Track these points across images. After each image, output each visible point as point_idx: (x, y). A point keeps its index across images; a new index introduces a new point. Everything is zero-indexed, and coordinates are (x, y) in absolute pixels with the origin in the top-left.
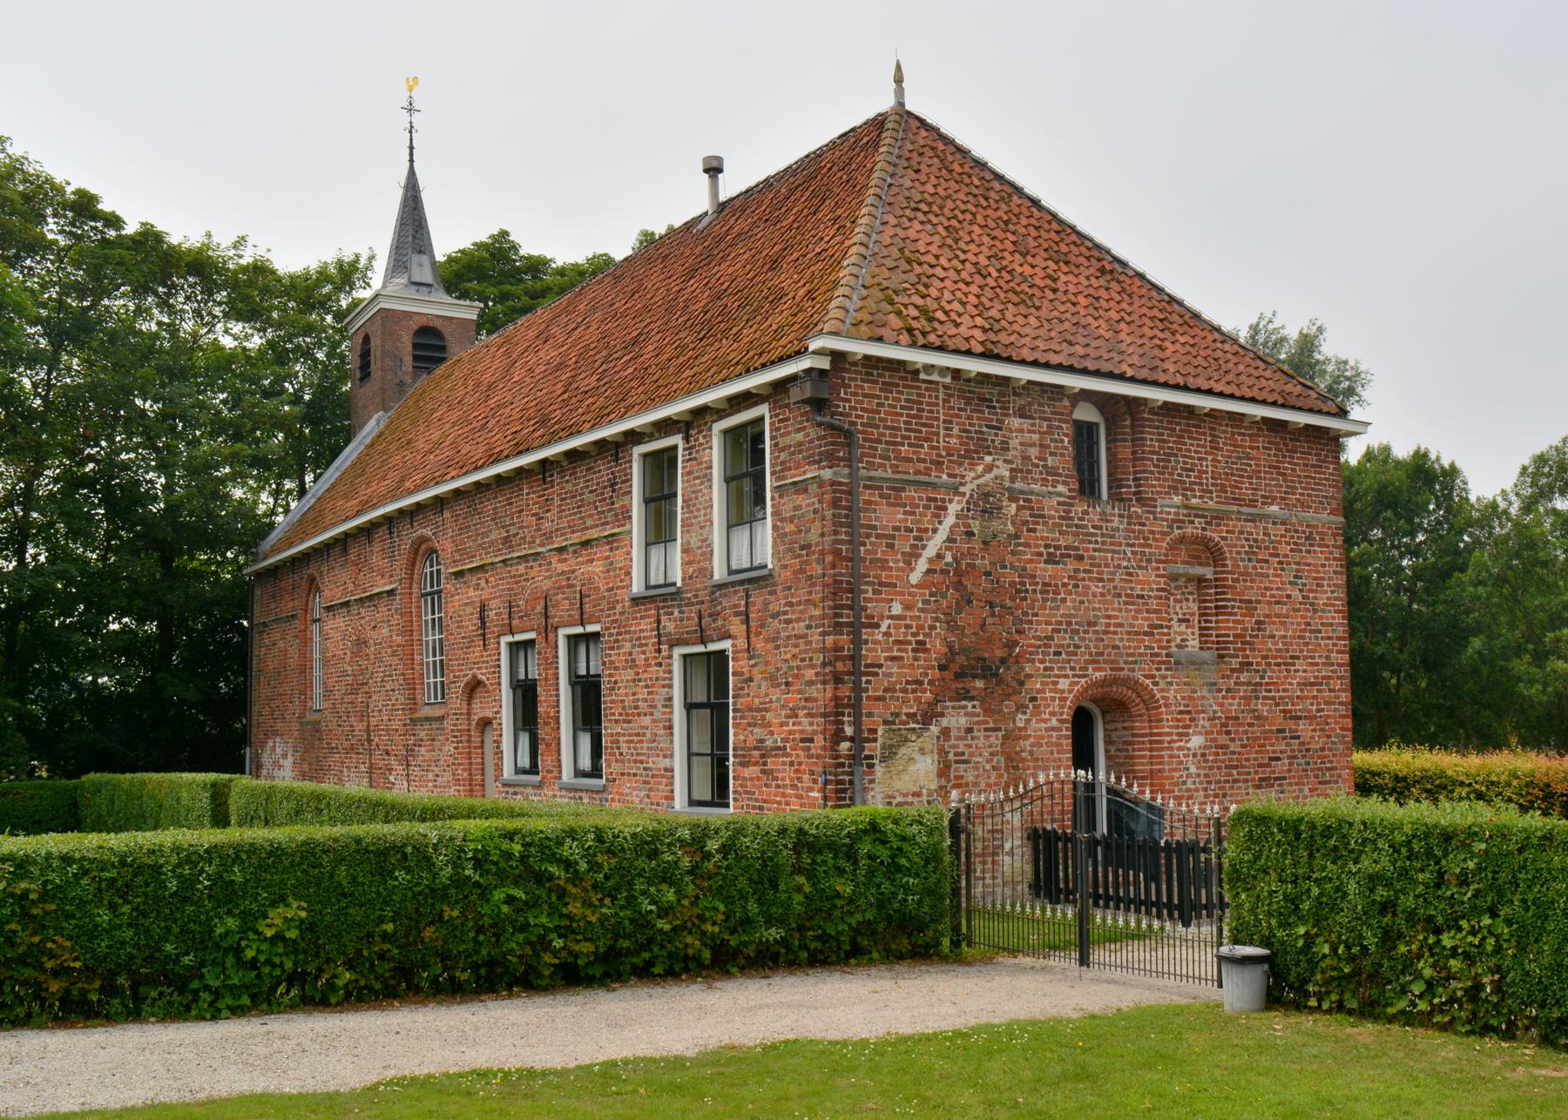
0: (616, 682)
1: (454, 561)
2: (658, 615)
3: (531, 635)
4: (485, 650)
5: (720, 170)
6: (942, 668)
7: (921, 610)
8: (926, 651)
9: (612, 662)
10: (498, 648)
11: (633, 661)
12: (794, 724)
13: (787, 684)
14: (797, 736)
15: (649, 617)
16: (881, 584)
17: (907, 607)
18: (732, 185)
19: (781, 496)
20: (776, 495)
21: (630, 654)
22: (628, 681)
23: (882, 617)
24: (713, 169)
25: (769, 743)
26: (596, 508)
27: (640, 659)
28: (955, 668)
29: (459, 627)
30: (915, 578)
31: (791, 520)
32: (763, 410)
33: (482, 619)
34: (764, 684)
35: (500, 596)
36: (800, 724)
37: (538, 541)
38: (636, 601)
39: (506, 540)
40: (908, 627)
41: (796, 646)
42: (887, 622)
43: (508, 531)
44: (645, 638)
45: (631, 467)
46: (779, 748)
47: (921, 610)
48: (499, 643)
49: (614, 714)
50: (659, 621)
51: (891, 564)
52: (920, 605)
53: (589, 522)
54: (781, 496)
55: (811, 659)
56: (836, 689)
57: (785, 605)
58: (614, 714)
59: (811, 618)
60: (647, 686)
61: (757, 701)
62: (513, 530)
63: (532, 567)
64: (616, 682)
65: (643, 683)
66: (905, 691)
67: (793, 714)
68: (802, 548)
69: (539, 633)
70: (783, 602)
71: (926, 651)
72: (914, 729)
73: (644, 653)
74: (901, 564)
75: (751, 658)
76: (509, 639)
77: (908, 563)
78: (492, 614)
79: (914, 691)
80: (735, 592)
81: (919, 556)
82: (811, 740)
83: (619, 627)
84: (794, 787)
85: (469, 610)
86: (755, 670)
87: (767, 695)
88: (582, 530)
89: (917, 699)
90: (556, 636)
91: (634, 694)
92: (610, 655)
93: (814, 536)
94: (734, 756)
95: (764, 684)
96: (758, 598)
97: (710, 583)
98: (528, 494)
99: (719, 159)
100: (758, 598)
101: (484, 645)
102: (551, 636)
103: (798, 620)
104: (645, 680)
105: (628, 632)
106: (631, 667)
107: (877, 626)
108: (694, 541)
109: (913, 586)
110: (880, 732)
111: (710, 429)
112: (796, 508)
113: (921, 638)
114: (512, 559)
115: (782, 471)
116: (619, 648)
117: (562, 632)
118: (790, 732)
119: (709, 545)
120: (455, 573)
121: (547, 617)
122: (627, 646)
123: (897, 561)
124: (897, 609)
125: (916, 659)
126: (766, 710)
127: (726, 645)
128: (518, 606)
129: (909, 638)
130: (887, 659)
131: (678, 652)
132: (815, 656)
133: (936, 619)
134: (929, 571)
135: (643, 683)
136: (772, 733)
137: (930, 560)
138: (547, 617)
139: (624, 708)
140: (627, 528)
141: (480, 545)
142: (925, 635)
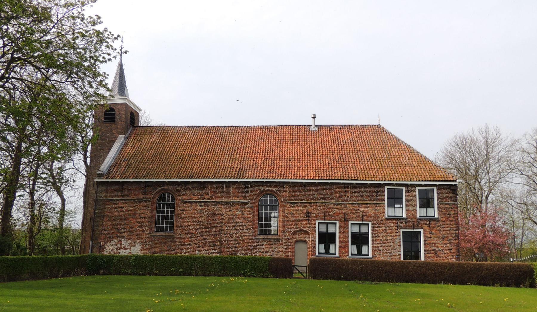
5: (315, 117)
14: (447, 249)
18: (318, 122)
20: (439, 204)
24: (314, 117)
25: (437, 250)
31: (444, 209)
32: (435, 188)
34: (435, 239)
37: (340, 200)
45: (384, 190)
50: (397, 224)
59: (451, 228)
61: (433, 242)
62: (327, 196)
67: (446, 244)
68: (448, 215)
75: (430, 233)
76: (323, 221)
80: (425, 221)
82: (452, 250)
84: (446, 258)
86: (432, 236)
87: (436, 241)
95: (435, 239)
99: (316, 115)
100: (433, 223)
108: (410, 209)
111: (416, 188)
112: (445, 207)
117: (350, 223)
118: (445, 248)
127: (422, 231)
131: (402, 230)
136: (438, 248)
140: (383, 202)
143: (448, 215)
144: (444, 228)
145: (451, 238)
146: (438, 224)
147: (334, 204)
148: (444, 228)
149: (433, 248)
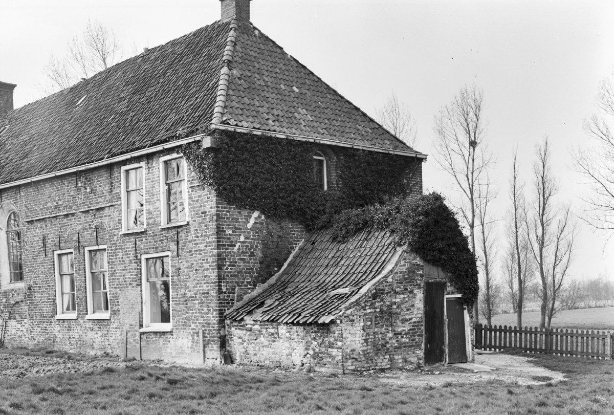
0: (115, 271)
1: (27, 216)
2: (136, 241)
3: (72, 250)
4: (46, 257)
6: (261, 263)
7: (252, 239)
8: (254, 256)
9: (112, 262)
10: (53, 256)
11: (123, 261)
12: (200, 287)
13: (196, 270)
15: (131, 242)
16: (236, 228)
17: (246, 238)
19: (192, 191)
20: (190, 191)
21: (122, 258)
22: (121, 270)
23: (236, 242)
25: (189, 295)
26: (103, 193)
27: (127, 261)
28: (266, 263)
29: (31, 247)
30: (249, 226)
33: (44, 243)
35: (54, 233)
36: (202, 286)
37: (73, 208)
38: (125, 235)
39: (56, 207)
40: (247, 246)
41: (200, 254)
42: (239, 244)
43: (57, 203)
44: (129, 251)
46: (193, 297)
47: (252, 239)
48: (53, 254)
49: (114, 285)
50: (136, 245)
51: (240, 220)
52: (252, 237)
53: (100, 200)
54: (192, 191)
55: (207, 260)
56: (218, 272)
57: (195, 237)
58: (114, 285)
60: (130, 272)
62: (60, 203)
63: (70, 220)
64: (115, 271)
65: (128, 271)
66: (246, 272)
68: (202, 213)
69: (75, 249)
70: (194, 236)
71: (254, 256)
72: (250, 288)
73: (128, 258)
74: (244, 220)
76: (59, 252)
77: (247, 220)
78: (49, 241)
79: (250, 273)
81: (251, 216)
82: (208, 293)
83: (116, 246)
85: (36, 239)
88: (97, 203)
89: (251, 276)
90: (84, 251)
91: (124, 276)
92: (112, 259)
93: (207, 209)
94: (172, 301)
96: (182, 235)
97: (160, 227)
98: (68, 186)
101: (46, 255)
102: (82, 251)
103: (201, 243)
104: (129, 269)
105: (121, 249)
106: (122, 264)
107: (235, 246)
109: (249, 229)
110: (236, 289)
113: (252, 250)
114: (60, 216)
115: (193, 180)
116: (116, 256)
117: (87, 249)
118: (198, 290)
119: (159, 211)
120: (28, 222)
121: (79, 242)
122: (120, 255)
123: (242, 219)
124: (242, 239)
125: (250, 259)
126: (187, 281)
128: (64, 237)
129: (248, 251)
130: (238, 259)
131: (144, 257)
132: (209, 258)
133: (258, 243)
134: (255, 223)
135: (128, 271)
137: (256, 218)
138: (79, 242)
139: (119, 282)
141: (42, 209)
142: (254, 250)
143: (202, 213)
144: (197, 244)
145: (206, 266)
146: (189, 238)
147: (67, 216)
148: (197, 244)
149: (183, 291)
